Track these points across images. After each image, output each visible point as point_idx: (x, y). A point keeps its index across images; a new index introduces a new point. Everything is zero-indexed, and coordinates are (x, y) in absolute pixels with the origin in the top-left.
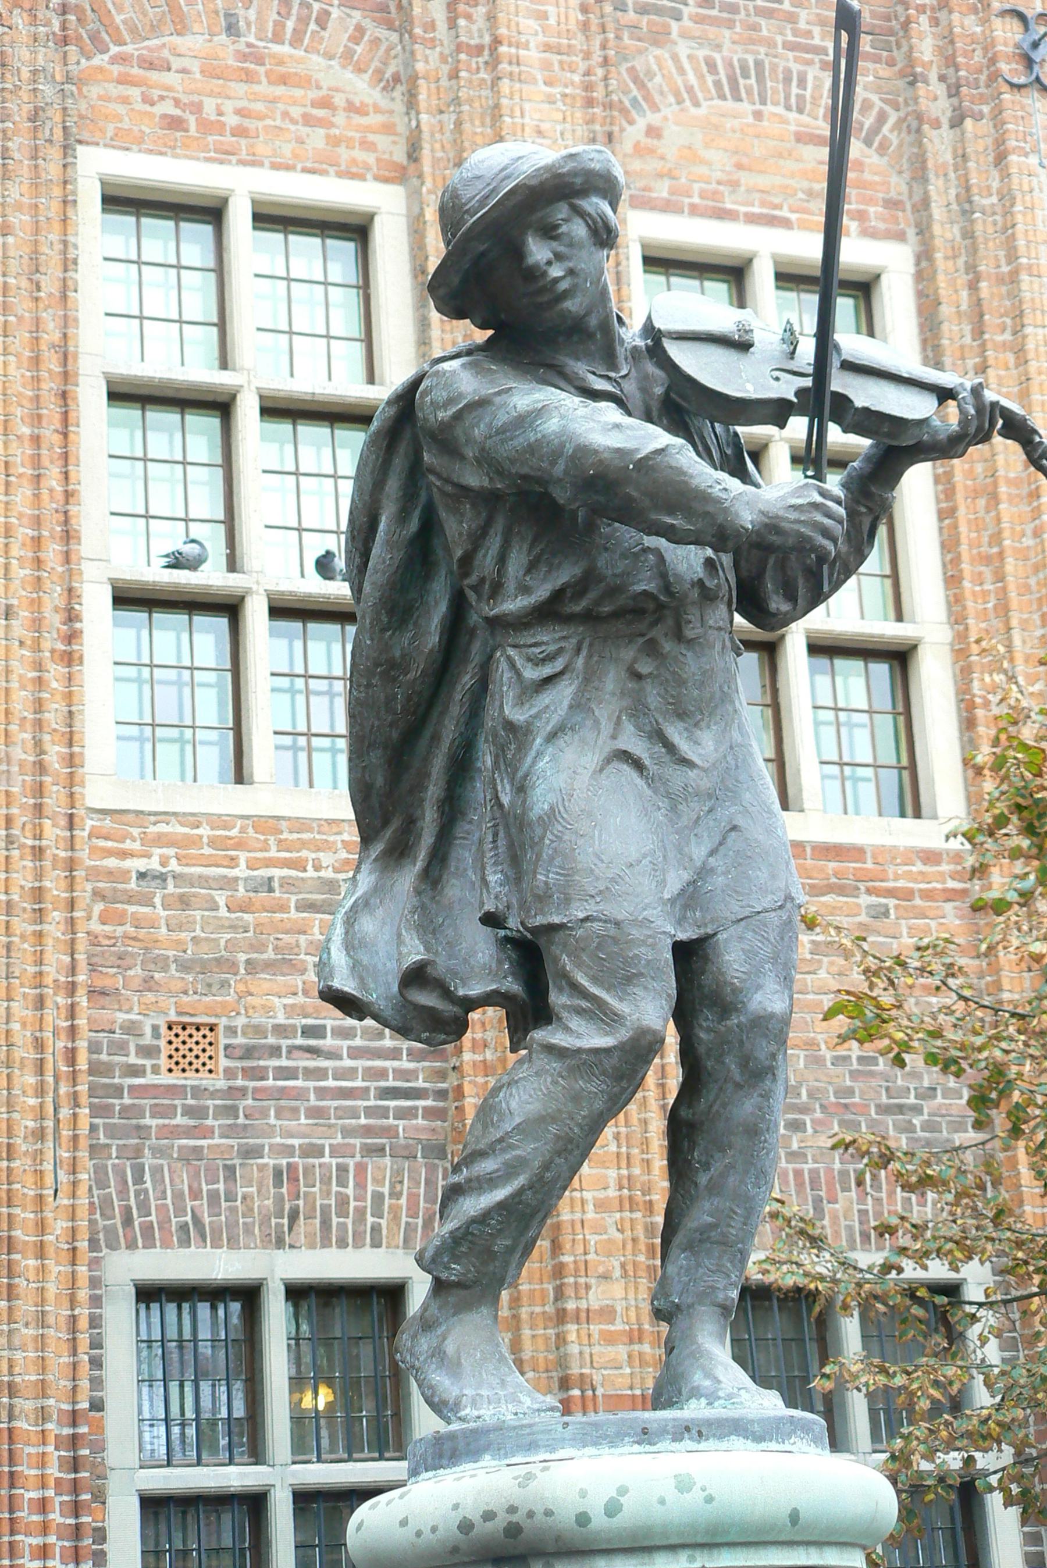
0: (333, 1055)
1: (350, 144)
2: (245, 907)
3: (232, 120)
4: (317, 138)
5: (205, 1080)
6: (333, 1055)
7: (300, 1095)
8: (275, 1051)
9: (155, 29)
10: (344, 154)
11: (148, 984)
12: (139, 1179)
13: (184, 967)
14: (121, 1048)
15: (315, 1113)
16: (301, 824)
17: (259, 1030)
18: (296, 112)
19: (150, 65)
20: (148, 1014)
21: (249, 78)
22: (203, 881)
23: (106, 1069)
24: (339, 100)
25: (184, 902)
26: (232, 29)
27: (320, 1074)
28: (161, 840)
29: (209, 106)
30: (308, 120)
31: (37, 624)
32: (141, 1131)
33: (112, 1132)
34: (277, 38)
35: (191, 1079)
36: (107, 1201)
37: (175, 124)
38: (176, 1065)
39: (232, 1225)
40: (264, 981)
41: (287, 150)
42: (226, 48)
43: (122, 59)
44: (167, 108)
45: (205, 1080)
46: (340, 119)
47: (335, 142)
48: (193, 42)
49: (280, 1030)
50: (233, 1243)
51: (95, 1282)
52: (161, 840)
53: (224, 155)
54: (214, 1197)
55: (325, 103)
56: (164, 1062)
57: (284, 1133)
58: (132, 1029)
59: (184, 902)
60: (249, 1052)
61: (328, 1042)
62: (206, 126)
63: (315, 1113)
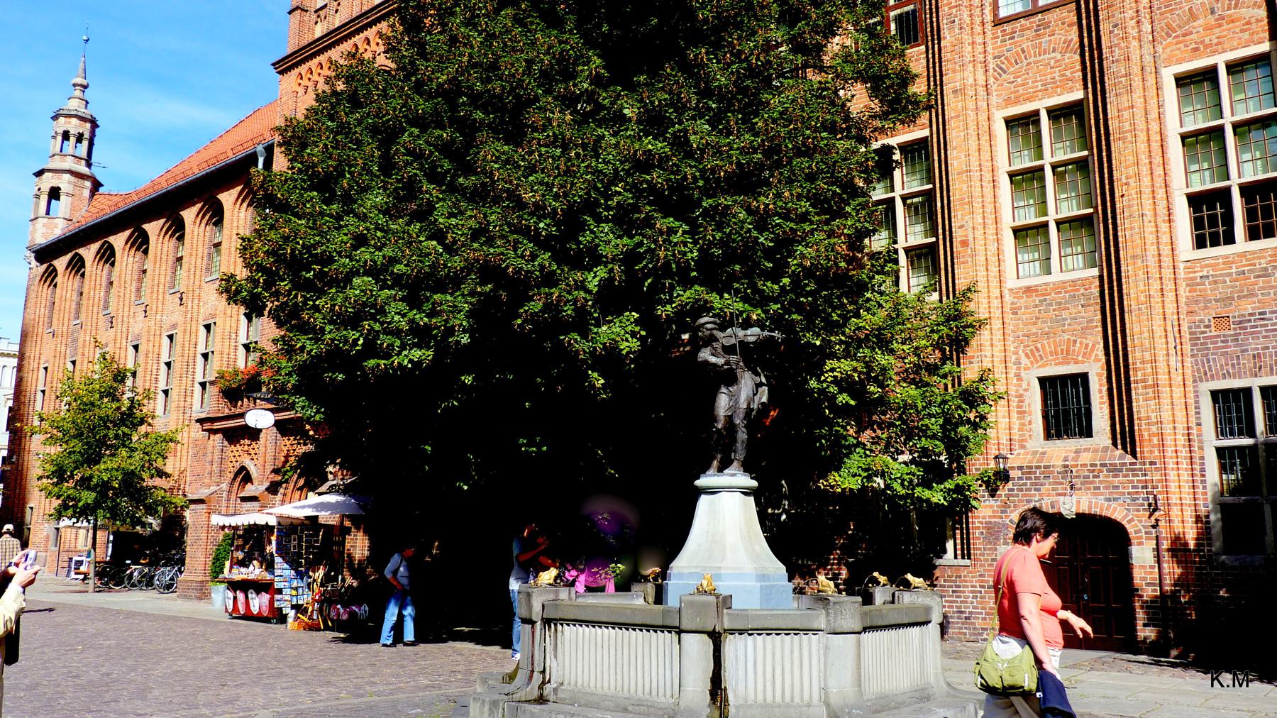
0: (1270, 319)
1: (1257, 33)
2: (1236, 281)
3: (1215, 41)
4: (1246, 35)
5: (1227, 332)
6: (1270, 319)
7: (1260, 332)
8: (1250, 321)
9: (1187, 22)
10: (1256, 37)
11: (1206, 308)
12: (1208, 361)
13: (1216, 301)
14: (1199, 327)
15: (1264, 337)
16: (1254, 252)
17: (1243, 316)
18: (1238, 30)
19: (1186, 35)
20: (1207, 316)
21: (1220, 25)
22: (1221, 275)
23: (1195, 333)
24: (1253, 20)
25: (1216, 282)
26: (1213, 12)
27: (1267, 325)
28: (1206, 266)
29: (1207, 41)
30: (1242, 31)
31: (1155, 215)
32: (1208, 349)
33: (1199, 350)
34: (1229, 9)
35: (1222, 333)
36: (1199, 370)
37: (1196, 49)
38: (1217, 328)
39: (1239, 372)
40: (1244, 301)
41: (1235, 43)
42: (1211, 19)
43: (1177, 37)
44: (1193, 46)
45: (1227, 332)
46: (1254, 26)
47: (1252, 34)
48: (1201, 22)
49: (1250, 315)
50: (1240, 377)
51: (1196, 392)
52: (1206, 266)
53: (1214, 53)
54: (1233, 365)
55: (1248, 23)
56: (1213, 328)
57: (1254, 344)
58: (1201, 321)
59: (1216, 282)
60: (1240, 322)
61: (1268, 316)
62: (1206, 47)
63: (1264, 337)
